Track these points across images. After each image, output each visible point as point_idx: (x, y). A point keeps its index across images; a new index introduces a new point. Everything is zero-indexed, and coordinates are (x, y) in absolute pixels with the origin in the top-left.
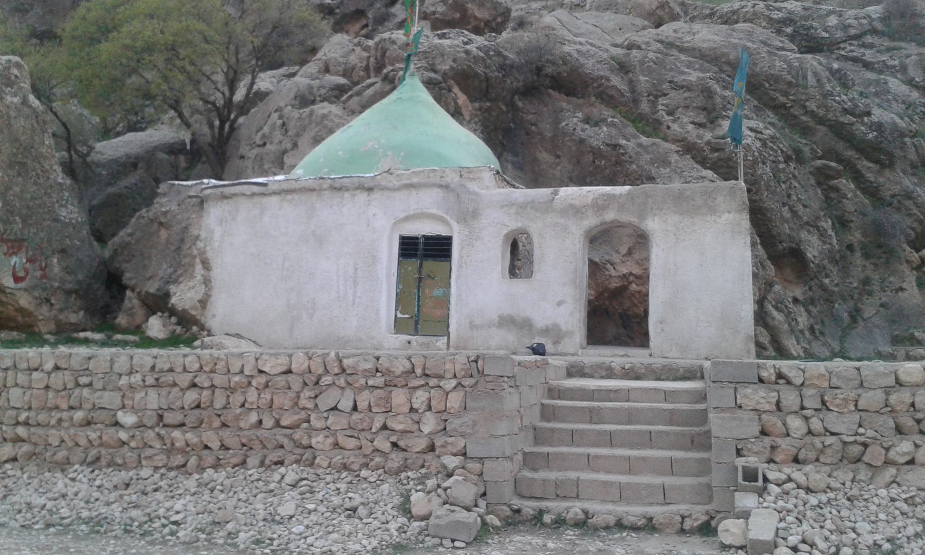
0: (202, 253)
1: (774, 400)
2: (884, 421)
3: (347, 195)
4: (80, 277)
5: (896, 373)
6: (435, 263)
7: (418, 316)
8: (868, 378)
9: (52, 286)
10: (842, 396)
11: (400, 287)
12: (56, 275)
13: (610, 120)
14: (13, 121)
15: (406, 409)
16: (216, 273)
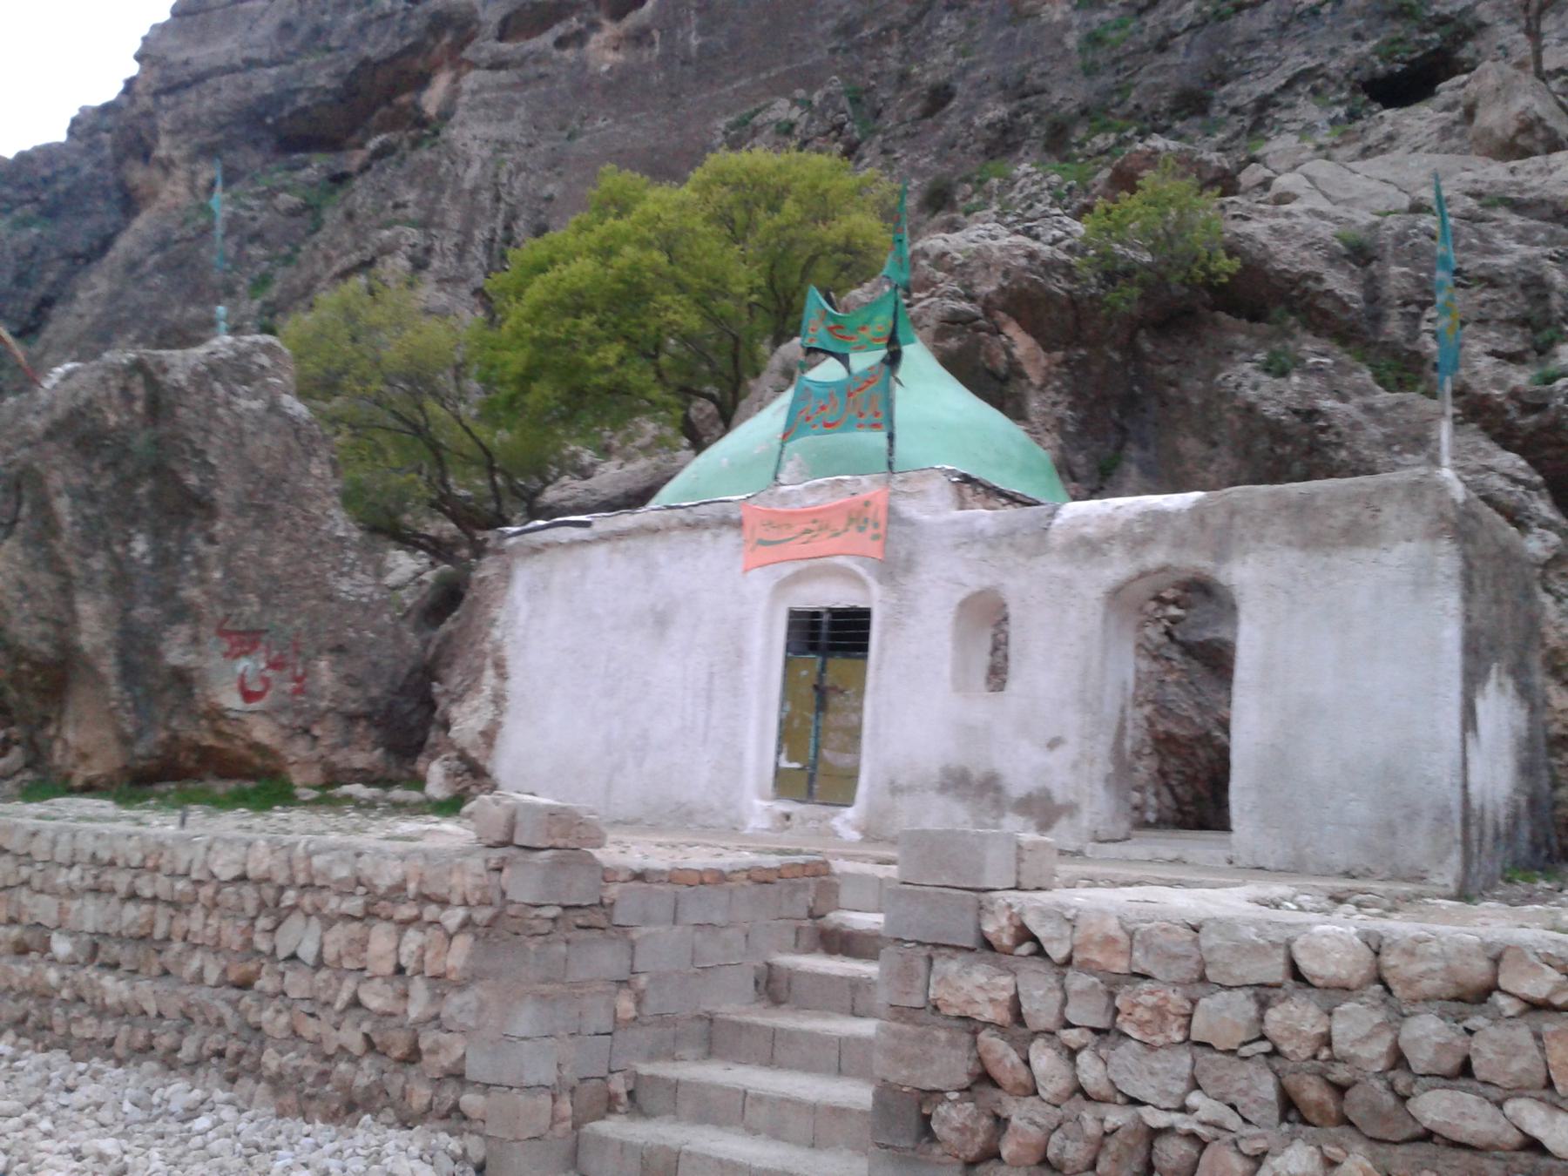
0: (498, 648)
1: (1005, 995)
2: (1249, 1078)
3: (707, 536)
4: (375, 692)
5: (1288, 946)
6: (847, 661)
7: (814, 767)
8: (1217, 956)
9: (314, 707)
10: (1150, 1000)
11: (788, 707)
12: (324, 688)
13: (1313, 360)
14: (248, 439)
15: (387, 967)
16: (514, 685)
